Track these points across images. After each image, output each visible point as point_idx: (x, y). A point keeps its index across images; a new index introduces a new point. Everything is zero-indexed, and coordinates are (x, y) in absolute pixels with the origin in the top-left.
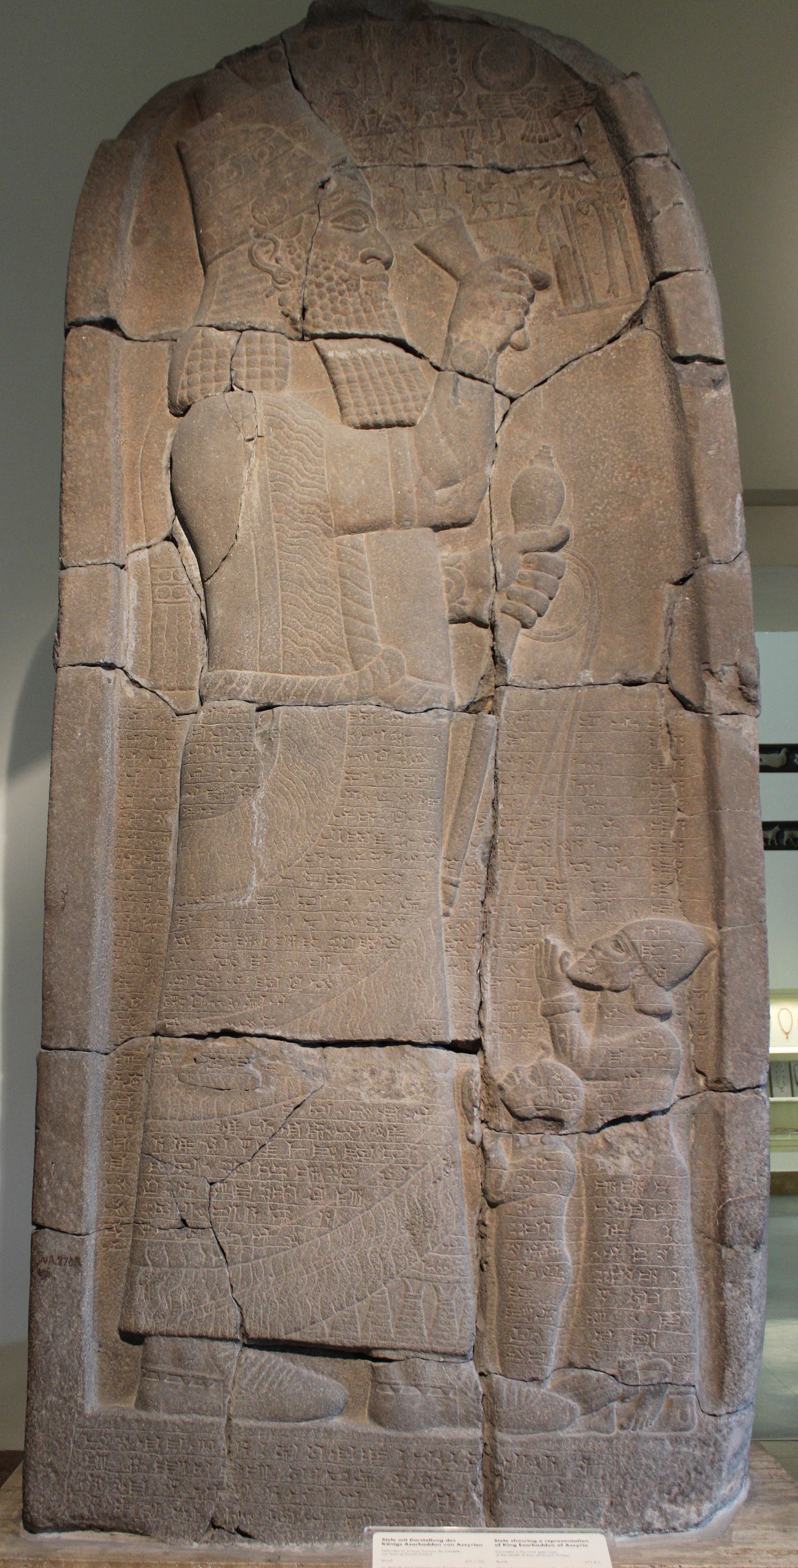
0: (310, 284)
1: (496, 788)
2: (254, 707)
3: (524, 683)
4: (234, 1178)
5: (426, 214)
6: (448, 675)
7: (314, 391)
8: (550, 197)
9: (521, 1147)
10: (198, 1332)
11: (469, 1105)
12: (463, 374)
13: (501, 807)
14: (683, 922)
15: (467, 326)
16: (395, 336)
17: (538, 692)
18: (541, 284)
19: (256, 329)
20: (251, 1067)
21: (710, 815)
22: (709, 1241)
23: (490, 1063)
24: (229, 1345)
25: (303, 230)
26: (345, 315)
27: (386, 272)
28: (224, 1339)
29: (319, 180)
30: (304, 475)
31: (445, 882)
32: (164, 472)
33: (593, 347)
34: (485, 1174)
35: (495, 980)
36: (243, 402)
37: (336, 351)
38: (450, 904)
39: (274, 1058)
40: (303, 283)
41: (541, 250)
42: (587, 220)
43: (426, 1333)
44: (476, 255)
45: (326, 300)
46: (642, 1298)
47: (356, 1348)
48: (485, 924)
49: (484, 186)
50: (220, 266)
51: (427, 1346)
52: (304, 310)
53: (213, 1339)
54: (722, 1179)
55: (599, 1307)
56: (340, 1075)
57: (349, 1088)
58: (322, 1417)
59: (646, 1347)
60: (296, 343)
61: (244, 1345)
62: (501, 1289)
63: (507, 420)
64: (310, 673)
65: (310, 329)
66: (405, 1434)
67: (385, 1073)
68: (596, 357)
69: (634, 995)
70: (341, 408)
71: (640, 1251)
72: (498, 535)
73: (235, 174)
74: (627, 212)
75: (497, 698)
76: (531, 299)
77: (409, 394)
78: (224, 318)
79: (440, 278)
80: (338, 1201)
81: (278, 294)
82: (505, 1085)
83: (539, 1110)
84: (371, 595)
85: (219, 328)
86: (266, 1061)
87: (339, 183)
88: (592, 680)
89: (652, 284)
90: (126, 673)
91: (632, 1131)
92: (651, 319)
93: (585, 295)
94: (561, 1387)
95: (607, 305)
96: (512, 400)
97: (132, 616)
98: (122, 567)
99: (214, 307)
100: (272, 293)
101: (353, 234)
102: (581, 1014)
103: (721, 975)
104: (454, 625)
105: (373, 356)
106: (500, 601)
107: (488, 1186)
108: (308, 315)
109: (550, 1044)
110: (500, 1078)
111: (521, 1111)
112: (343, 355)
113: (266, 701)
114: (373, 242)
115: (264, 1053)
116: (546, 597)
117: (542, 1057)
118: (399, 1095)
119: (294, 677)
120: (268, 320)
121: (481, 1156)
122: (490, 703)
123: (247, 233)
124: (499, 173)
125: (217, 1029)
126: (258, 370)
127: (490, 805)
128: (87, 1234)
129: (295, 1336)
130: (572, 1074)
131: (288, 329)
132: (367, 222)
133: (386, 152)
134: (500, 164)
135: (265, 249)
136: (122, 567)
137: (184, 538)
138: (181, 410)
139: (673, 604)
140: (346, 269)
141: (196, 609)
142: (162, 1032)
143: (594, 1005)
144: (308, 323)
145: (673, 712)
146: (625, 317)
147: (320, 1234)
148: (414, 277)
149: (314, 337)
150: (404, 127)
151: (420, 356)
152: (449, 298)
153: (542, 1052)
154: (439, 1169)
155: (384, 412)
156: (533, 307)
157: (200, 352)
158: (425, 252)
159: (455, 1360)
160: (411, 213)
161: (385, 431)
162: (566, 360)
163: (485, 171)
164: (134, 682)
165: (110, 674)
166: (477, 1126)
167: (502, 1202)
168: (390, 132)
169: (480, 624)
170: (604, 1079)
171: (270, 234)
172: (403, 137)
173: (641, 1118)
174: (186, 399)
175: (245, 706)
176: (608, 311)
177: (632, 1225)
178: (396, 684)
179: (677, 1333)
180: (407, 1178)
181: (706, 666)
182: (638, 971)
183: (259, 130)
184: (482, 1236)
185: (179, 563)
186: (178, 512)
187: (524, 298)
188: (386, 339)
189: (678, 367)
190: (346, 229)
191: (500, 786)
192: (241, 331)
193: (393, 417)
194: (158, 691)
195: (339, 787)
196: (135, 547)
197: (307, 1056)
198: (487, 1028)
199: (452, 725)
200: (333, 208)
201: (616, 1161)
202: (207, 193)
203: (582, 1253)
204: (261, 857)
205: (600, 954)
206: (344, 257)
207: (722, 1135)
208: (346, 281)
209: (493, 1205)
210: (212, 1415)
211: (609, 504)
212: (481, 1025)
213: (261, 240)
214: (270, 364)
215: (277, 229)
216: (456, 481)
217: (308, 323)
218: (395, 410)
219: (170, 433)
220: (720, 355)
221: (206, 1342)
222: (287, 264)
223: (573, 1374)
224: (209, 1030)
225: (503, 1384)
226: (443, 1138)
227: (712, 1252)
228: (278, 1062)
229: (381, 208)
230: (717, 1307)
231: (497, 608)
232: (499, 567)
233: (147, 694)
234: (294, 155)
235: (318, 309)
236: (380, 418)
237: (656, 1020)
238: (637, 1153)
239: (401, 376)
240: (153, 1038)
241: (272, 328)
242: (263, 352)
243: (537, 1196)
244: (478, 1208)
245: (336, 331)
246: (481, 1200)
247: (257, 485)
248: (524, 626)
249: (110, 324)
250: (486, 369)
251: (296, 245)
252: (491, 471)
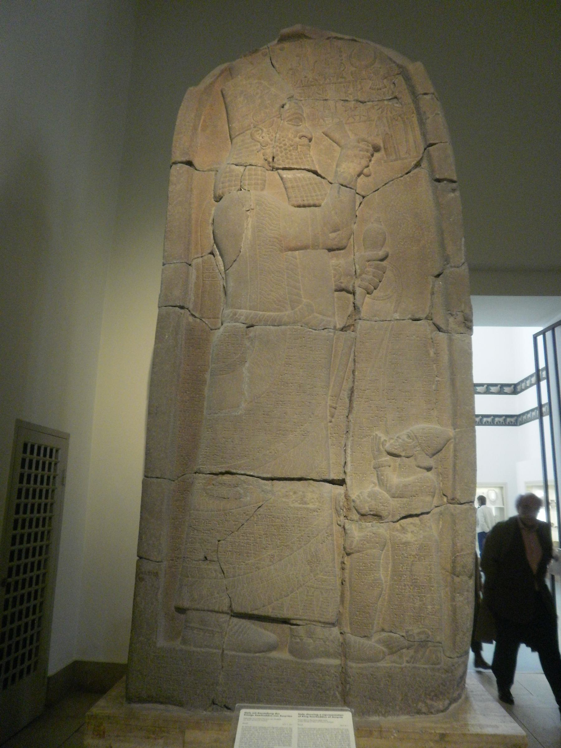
1: (355, 365)
2: (245, 326)
3: (368, 319)
4: (229, 538)
6: (334, 314)
8: (382, 113)
9: (362, 528)
10: (211, 609)
11: (339, 509)
12: (342, 185)
13: (356, 373)
14: (438, 427)
15: (344, 165)
16: (313, 169)
17: (374, 323)
18: (377, 149)
19: (252, 165)
20: (239, 488)
21: (451, 379)
22: (447, 573)
23: (349, 489)
24: (225, 615)
28: (223, 612)
29: (281, 104)
30: (271, 226)
31: (331, 407)
32: (210, 225)
33: (399, 176)
34: (345, 540)
35: (353, 452)
37: (287, 175)
38: (333, 417)
39: (249, 484)
41: (377, 135)
42: (397, 123)
43: (316, 612)
44: (349, 137)
45: (283, 154)
46: (417, 599)
47: (284, 619)
48: (348, 426)
49: (353, 109)
50: (237, 140)
51: (316, 619)
52: (273, 158)
53: (217, 612)
54: (454, 544)
55: (396, 603)
56: (280, 493)
57: (284, 500)
58: (267, 651)
59: (419, 623)
60: (270, 172)
61: (232, 616)
62: (351, 594)
63: (361, 205)
64: (272, 311)
65: (276, 166)
66: (305, 661)
67: (301, 493)
68: (401, 180)
69: (415, 459)
70: (289, 198)
71: (416, 577)
72: (357, 254)
73: (246, 101)
74: (415, 119)
75: (356, 325)
76: (372, 155)
77: (319, 193)
79: (333, 146)
80: (277, 551)
81: (262, 151)
82: (356, 499)
83: (371, 511)
84: (300, 277)
85: (236, 165)
86: (246, 486)
88: (398, 318)
89: (425, 149)
90: (189, 311)
91: (414, 522)
92: (424, 164)
93: (396, 153)
94: (379, 641)
95: (406, 158)
96: (364, 197)
97: (193, 286)
98: (190, 265)
99: (235, 156)
100: (260, 151)
101: (295, 127)
102: (391, 467)
103: (455, 450)
104: (337, 293)
105: (303, 178)
106: (358, 282)
107: (346, 546)
108: (275, 160)
109: (376, 481)
110: (353, 497)
111: (363, 511)
112: (290, 176)
113: (250, 323)
115: (245, 482)
116: (378, 281)
117: (373, 487)
118: (306, 503)
119: (264, 313)
121: (343, 532)
122: (352, 328)
123: (250, 125)
124: (359, 103)
125: (223, 470)
127: (351, 372)
128: (161, 562)
129: (256, 612)
130: (387, 495)
131: (267, 166)
134: (360, 99)
135: (258, 133)
136: (190, 265)
137: (218, 253)
138: (218, 199)
139: (434, 285)
140: (292, 141)
141: (221, 283)
142: (198, 471)
143: (397, 464)
145: (434, 333)
146: (413, 164)
147: (268, 566)
149: (277, 169)
151: (324, 178)
152: (337, 155)
153: (373, 485)
154: (324, 537)
155: (308, 200)
156: (373, 159)
157: (228, 174)
158: (327, 135)
159: (329, 626)
160: (321, 120)
161: (308, 209)
162: (388, 181)
163: (353, 102)
164: (193, 315)
165: (182, 311)
166: (342, 518)
167: (352, 553)
169: (348, 292)
170: (401, 498)
171: (260, 126)
173: (417, 515)
174: (221, 194)
175: (242, 325)
176: (406, 161)
177: (412, 565)
178: (310, 317)
179: (433, 617)
180: (309, 541)
181: (449, 312)
182: (418, 449)
184: (343, 569)
185: (215, 264)
186: (215, 242)
187: (369, 154)
188: (309, 171)
189: (437, 183)
191: (357, 364)
192: (246, 166)
193: (312, 202)
194: (203, 319)
195: (283, 363)
196: (196, 256)
197: (265, 485)
198: (348, 474)
199: (335, 336)
201: (406, 535)
203: (389, 578)
204: (246, 393)
205: (400, 440)
207: (455, 524)
208: (292, 146)
209: (348, 554)
210: (216, 649)
211: (406, 242)
212: (345, 472)
213: (256, 129)
214: (258, 180)
216: (339, 230)
217: (275, 163)
219: (213, 209)
220: (455, 178)
221: (215, 614)
222: (267, 138)
223: (384, 635)
224: (220, 471)
225: (352, 638)
226: (326, 523)
227: (449, 579)
228: (251, 486)
230: (452, 605)
231: (356, 285)
232: (357, 267)
233: (198, 320)
235: (279, 157)
236: (306, 203)
237: (425, 471)
238: (415, 531)
240: (194, 475)
241: (259, 165)
242: (255, 175)
243: (369, 551)
244: (341, 556)
245: (287, 166)
246: (343, 552)
247: (250, 230)
248: (368, 293)
249: (190, 163)
250: (353, 183)
251: (271, 131)
252: (355, 227)
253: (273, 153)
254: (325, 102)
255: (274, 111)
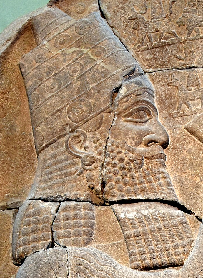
0: (107, 165)
5: (194, 105)
7: (111, 243)
16: (169, 199)
19: (70, 200)
25: (103, 125)
26: (132, 186)
27: (164, 152)
29: (114, 87)
36: (59, 255)
37: (128, 212)
40: (103, 164)
45: (119, 177)
52: (103, 184)
60: (100, 208)
73: (57, 86)
78: (49, 193)
81: (86, 174)
85: (45, 200)
87: (128, 88)
100: (81, 173)
105: (153, 216)
108: (107, 188)
112: (131, 216)
114: (154, 130)
120: (79, 192)
126: (72, 231)
132: (149, 115)
133: (165, 60)
135: (77, 140)
144: (107, 193)
148: (185, 153)
150: (179, 40)
151: (189, 212)
160: (183, 104)
168: (169, 45)
171: (81, 130)
172: (178, 48)
183: (73, 53)
190: (134, 122)
192: (60, 202)
193: (167, 260)
200: (124, 107)
202: (38, 102)
206: (131, 143)
208: (132, 161)
214: (80, 226)
215: (86, 126)
217: (107, 193)
218: (169, 255)
229: (161, 102)
234: (97, 69)
236: (157, 261)
239: (172, 230)
241: (82, 198)
242: (75, 217)
245: (126, 198)
251: (98, 136)
253: (102, 175)
254: (190, 70)
255: (102, 101)
